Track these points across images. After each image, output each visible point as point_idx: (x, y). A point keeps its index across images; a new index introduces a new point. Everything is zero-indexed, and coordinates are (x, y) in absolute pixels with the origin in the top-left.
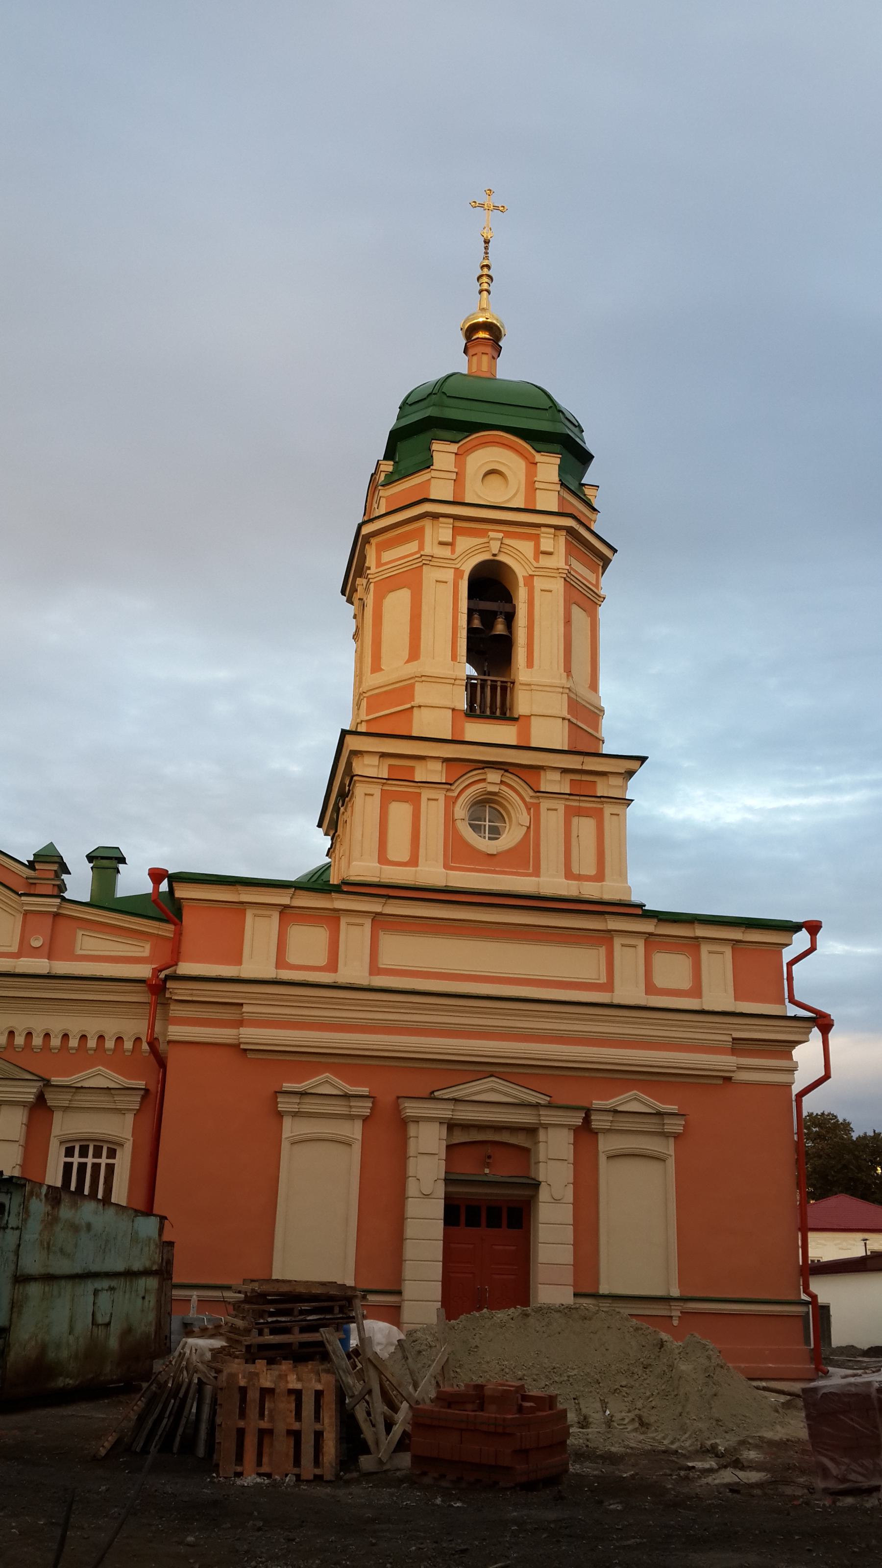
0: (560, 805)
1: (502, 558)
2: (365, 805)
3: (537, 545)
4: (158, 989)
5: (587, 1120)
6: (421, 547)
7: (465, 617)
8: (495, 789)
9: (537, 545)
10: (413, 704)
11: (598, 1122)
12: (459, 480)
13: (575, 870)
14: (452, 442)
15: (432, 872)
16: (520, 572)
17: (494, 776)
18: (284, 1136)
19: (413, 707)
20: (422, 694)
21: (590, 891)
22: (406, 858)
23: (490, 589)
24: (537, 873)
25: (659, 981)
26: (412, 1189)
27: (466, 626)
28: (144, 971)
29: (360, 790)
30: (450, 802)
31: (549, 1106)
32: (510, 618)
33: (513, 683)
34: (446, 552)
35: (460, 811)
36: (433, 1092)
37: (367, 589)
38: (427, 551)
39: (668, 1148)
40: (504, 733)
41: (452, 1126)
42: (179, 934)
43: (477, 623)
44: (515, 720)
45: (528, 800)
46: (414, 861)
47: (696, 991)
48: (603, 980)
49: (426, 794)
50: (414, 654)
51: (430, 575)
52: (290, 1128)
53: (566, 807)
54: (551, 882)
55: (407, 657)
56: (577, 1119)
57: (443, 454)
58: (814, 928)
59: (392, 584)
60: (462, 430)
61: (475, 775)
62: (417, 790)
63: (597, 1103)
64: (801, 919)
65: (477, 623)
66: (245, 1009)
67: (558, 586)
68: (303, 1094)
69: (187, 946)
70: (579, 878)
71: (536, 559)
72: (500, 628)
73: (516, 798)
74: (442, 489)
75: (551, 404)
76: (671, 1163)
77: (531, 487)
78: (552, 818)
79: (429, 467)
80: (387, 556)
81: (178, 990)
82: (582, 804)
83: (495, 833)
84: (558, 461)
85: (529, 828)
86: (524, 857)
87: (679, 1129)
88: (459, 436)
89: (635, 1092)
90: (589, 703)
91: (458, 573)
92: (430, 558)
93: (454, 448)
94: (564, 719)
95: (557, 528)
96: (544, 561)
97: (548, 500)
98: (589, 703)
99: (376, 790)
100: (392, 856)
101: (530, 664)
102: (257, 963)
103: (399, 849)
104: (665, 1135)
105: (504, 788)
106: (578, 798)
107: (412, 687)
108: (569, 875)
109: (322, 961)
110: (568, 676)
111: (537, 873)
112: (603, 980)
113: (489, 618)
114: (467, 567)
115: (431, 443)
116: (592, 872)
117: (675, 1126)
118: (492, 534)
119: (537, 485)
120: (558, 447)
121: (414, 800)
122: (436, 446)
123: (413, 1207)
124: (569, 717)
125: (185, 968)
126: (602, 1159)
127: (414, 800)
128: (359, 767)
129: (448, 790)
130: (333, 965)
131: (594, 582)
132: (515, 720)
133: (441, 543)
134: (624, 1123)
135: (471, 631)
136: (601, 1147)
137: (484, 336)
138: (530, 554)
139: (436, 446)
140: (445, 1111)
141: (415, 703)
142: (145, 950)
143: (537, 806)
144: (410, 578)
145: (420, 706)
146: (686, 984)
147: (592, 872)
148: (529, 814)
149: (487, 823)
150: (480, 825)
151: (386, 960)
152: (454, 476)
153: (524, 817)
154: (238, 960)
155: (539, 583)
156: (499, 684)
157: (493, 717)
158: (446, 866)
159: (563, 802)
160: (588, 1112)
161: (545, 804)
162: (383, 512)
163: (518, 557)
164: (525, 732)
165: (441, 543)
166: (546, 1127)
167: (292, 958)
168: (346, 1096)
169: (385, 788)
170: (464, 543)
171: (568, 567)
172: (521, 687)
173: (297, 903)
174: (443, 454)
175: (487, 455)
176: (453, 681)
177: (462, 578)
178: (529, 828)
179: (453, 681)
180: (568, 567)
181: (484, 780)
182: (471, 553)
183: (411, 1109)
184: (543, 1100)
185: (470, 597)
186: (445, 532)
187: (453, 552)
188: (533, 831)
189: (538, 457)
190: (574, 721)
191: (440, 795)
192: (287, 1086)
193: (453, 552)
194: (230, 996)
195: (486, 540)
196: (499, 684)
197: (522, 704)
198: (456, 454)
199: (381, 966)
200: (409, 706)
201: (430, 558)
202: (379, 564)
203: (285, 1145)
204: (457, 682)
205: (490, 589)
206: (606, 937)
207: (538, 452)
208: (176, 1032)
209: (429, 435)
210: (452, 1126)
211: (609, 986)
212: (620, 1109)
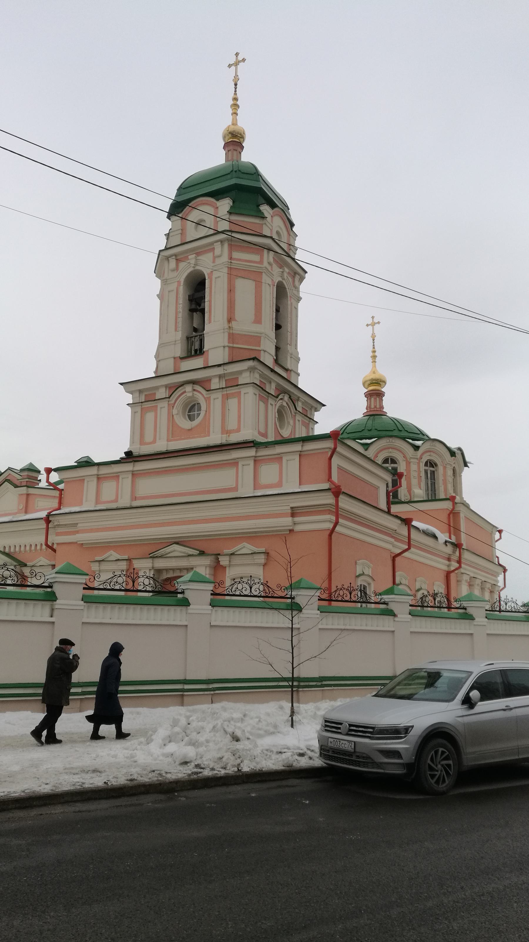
1: (198, 268)
16: (206, 272)
17: (188, 388)
45: (206, 396)
54: (215, 438)
66: (79, 525)
69: (64, 501)
73: (200, 396)
91: (179, 282)
98: (248, 332)
101: (210, 322)
105: (195, 393)
133: (173, 270)
155: (215, 274)
170: (182, 265)
182: (185, 270)
204: (177, 342)
206: (234, 463)
211: (236, 489)
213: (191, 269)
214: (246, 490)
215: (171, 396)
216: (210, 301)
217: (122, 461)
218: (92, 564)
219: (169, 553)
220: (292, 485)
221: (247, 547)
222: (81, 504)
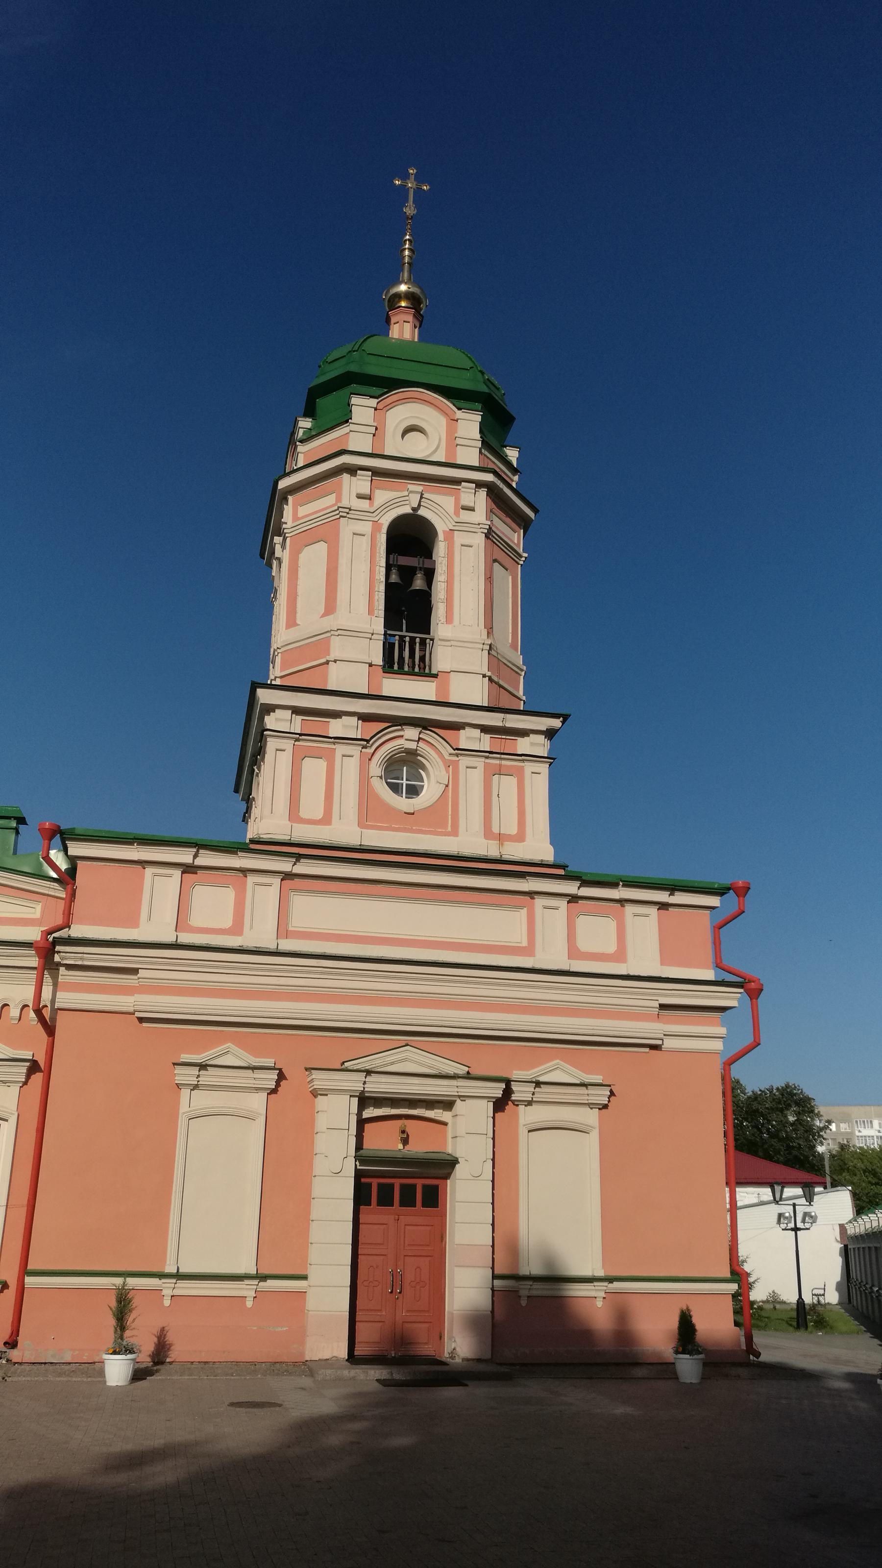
0: (479, 762)
1: (422, 512)
2: (277, 759)
4: (48, 952)
5: (508, 1092)
6: (339, 499)
7: (383, 570)
8: (413, 746)
9: (457, 500)
10: (328, 658)
11: (520, 1092)
12: (377, 433)
13: (496, 830)
14: (371, 397)
15: (346, 831)
16: (441, 526)
17: (411, 733)
18: (181, 1111)
19: (327, 662)
20: (338, 648)
21: (514, 851)
22: (319, 814)
23: (410, 542)
24: (455, 832)
25: (583, 945)
26: (321, 1166)
27: (383, 579)
28: (33, 934)
29: (272, 744)
31: (468, 1076)
32: (430, 574)
33: (432, 640)
34: (364, 504)
35: (376, 768)
36: (343, 1063)
37: (283, 546)
38: (345, 503)
39: (591, 1117)
41: (364, 1100)
42: (73, 895)
43: (394, 578)
44: (435, 676)
45: (447, 757)
46: (326, 819)
47: (620, 955)
48: (525, 944)
49: (341, 749)
50: (330, 608)
51: (347, 528)
52: (189, 1102)
53: (486, 766)
54: (470, 842)
55: (323, 611)
56: (497, 1090)
57: (362, 408)
58: (742, 891)
59: (310, 537)
61: (394, 731)
62: (333, 746)
63: (516, 1074)
64: (726, 882)
65: (394, 578)
66: (142, 973)
67: (479, 540)
68: (203, 1067)
70: (501, 838)
71: (457, 514)
72: (419, 583)
74: (360, 441)
75: (472, 365)
76: (595, 1135)
77: (452, 442)
78: (472, 774)
79: (347, 421)
80: (302, 511)
81: (65, 955)
82: (504, 762)
83: (413, 791)
84: (479, 418)
85: (447, 786)
86: (442, 816)
87: (605, 1100)
88: (379, 391)
89: (558, 1061)
90: (510, 662)
91: (376, 525)
92: (347, 510)
93: (373, 402)
94: (484, 676)
95: (479, 485)
96: (465, 516)
97: (470, 455)
98: (510, 662)
99: (288, 744)
100: (304, 814)
101: (449, 619)
102: (157, 925)
104: (591, 1106)
106: (498, 756)
107: (327, 641)
108: (488, 833)
109: (228, 923)
110: (488, 633)
111: (455, 832)
112: (525, 944)
113: (407, 573)
114: (386, 520)
115: (350, 398)
116: (514, 831)
117: (601, 1095)
118: (412, 487)
119: (458, 441)
120: (479, 406)
122: (355, 400)
123: (319, 1187)
124: (489, 674)
125: (77, 931)
126: (523, 1132)
128: (271, 721)
129: (364, 747)
130: (237, 929)
131: (516, 541)
132: (435, 676)
133: (360, 497)
134: (544, 1093)
135: (389, 586)
136: (522, 1121)
138: (451, 509)
139: (355, 400)
140: (355, 1083)
141: (331, 657)
142: (35, 911)
143: (456, 765)
144: (325, 532)
145: (335, 661)
146: (612, 948)
147: (514, 831)
148: (448, 772)
149: (405, 782)
150: (398, 784)
151: (297, 922)
152: (373, 430)
154: (134, 923)
155: (459, 538)
156: (418, 640)
157: (411, 673)
158: (360, 825)
159: (483, 759)
160: (508, 1082)
161: (464, 761)
162: (301, 464)
163: (440, 510)
164: (443, 688)
165: (360, 497)
166: (463, 1098)
167: (197, 919)
168: (254, 1068)
169: (296, 743)
170: (382, 496)
171: (489, 523)
172: (440, 643)
173: (199, 862)
174: (362, 408)
175: (407, 410)
176: (370, 636)
177: (380, 530)
178: (447, 786)
179: (370, 636)
180: (489, 523)
181: (402, 736)
183: (321, 1080)
184: (463, 1070)
185: (390, 550)
186: (362, 483)
187: (371, 505)
188: (451, 788)
189: (459, 414)
190: (495, 678)
191: (355, 750)
192: (185, 1058)
193: (371, 505)
194: (121, 959)
195: (406, 493)
196: (418, 640)
197: (442, 658)
198: (376, 409)
199: (291, 929)
200: (323, 660)
201: (347, 510)
202: (295, 517)
203: (182, 1122)
204: (374, 637)
205: (410, 542)
207: (459, 409)
208: (65, 999)
209: (347, 390)
210: (364, 1100)
211: (529, 950)
212: (541, 1079)
213: (407, 510)
214: (553, 955)
215: (372, 738)
216: (450, 583)
217: (252, 846)
218: (179, 1070)
219: (392, 1063)
220: (645, 959)
221: (558, 1070)
222: (134, 923)
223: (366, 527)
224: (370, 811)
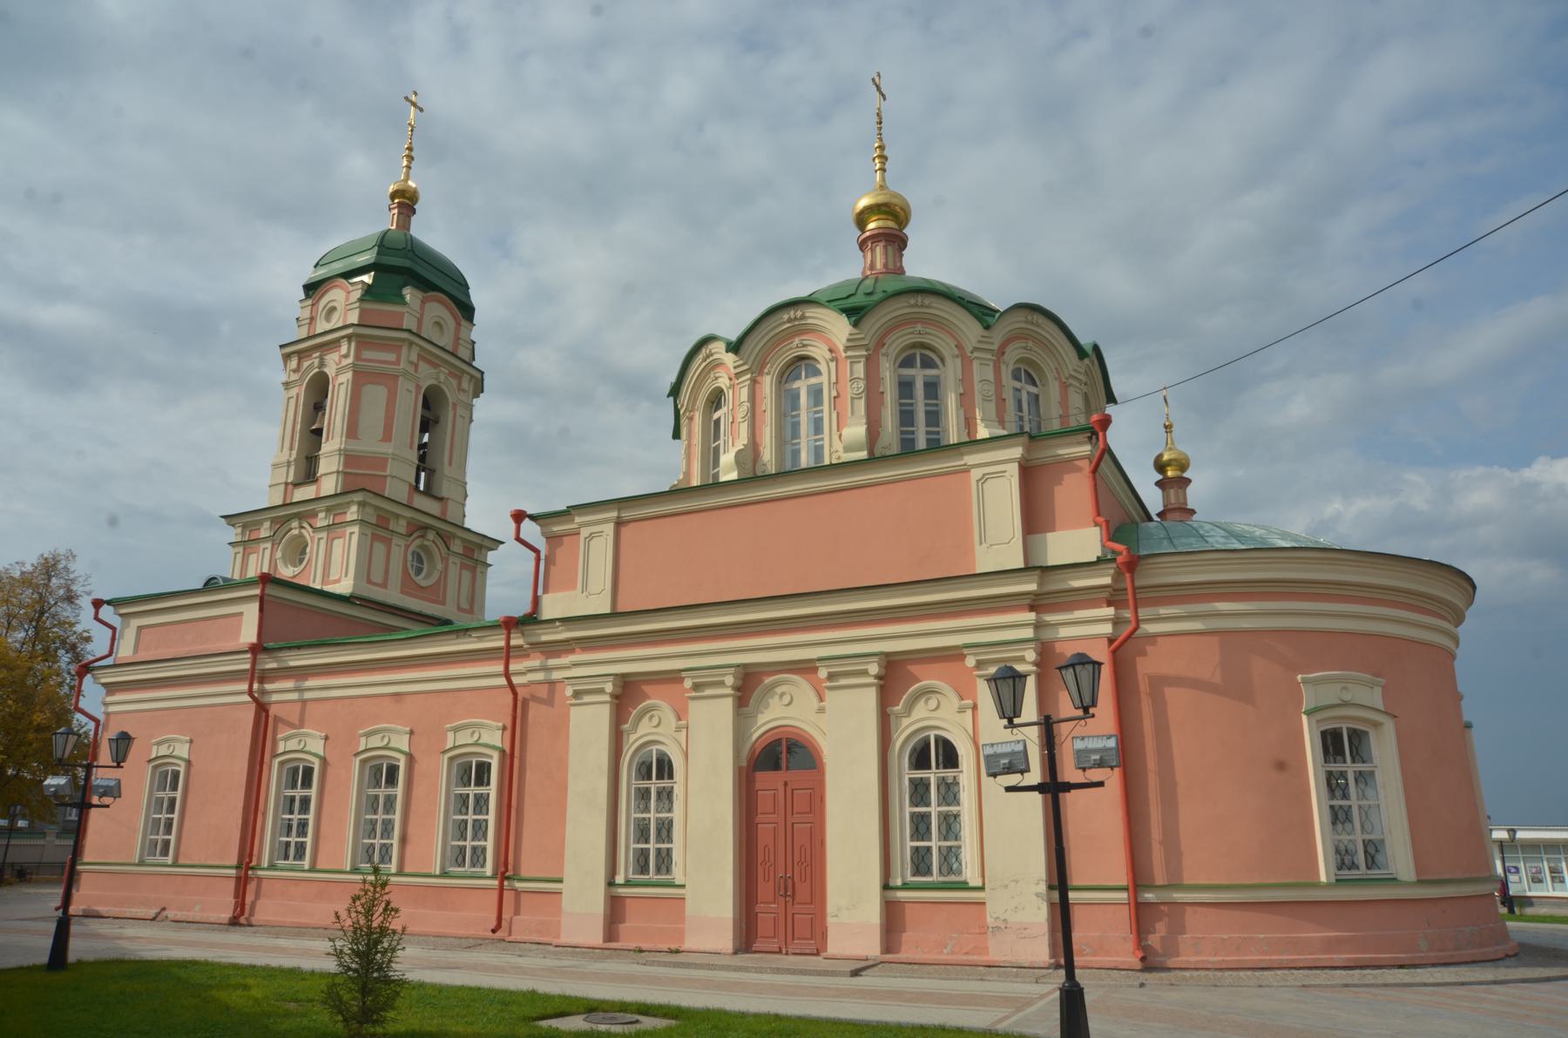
3: (460, 384)
15: (393, 596)
24: (443, 603)
30: (407, 547)
40: (432, 507)
46: (384, 585)
49: (395, 540)
60: (425, 285)
78: (453, 571)
93: (420, 295)
103: (377, 577)
111: (443, 603)
114: (425, 386)
121: (388, 542)
127: (388, 542)
137: (406, 202)
153: (440, 566)
161: (452, 559)
164: (444, 511)
191: (402, 543)
223: (412, 386)
224: (409, 586)
